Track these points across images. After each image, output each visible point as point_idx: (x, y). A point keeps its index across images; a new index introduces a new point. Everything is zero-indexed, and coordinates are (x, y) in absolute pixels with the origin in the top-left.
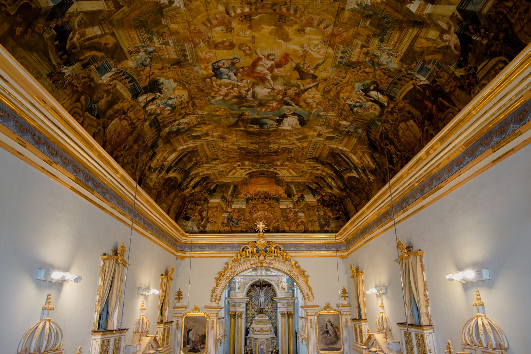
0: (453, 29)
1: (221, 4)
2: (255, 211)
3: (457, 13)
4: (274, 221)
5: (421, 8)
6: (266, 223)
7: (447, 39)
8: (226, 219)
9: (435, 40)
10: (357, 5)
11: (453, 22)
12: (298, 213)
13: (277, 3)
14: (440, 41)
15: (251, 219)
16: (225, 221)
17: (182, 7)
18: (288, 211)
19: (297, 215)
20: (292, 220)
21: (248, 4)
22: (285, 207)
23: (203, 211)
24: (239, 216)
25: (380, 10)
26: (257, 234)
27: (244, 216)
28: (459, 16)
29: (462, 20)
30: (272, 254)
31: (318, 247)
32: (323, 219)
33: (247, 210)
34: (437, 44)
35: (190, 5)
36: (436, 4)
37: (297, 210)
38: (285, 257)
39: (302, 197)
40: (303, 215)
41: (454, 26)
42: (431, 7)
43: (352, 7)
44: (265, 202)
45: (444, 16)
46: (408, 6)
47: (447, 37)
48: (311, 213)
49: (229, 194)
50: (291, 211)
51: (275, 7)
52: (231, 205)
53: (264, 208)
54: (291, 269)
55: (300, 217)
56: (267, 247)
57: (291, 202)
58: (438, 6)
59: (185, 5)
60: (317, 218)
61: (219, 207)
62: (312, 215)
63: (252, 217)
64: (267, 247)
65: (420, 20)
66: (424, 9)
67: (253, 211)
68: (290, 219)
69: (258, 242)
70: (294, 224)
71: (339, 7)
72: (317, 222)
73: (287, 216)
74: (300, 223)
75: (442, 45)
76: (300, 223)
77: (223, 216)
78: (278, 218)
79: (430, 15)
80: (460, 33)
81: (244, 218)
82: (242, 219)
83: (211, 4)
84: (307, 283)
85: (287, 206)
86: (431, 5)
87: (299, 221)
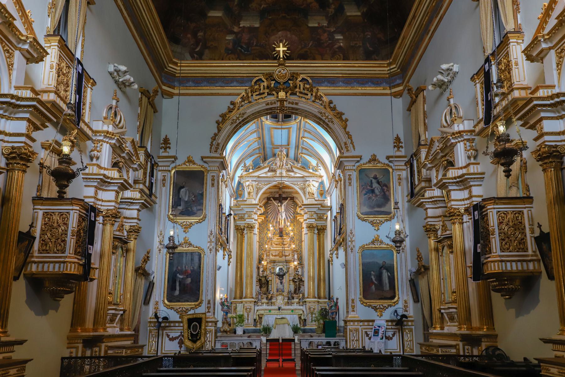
4: (300, 47)
6: (289, 46)
16: (230, 46)
19: (334, 37)
20: (326, 45)
26: (276, 61)
31: (362, 80)
37: (332, 30)
38: (314, 94)
39: (340, 10)
40: (342, 37)
44: (288, 17)
49: (236, 3)
52: (239, 22)
56: (289, 80)
57: (324, 18)
64: (289, 80)
69: (277, 72)
70: (328, 51)
72: (361, 49)
74: (337, 50)
76: (337, 50)
77: (227, 38)
82: (255, 44)
84: (345, 128)
85: (319, 24)
87: (336, 46)
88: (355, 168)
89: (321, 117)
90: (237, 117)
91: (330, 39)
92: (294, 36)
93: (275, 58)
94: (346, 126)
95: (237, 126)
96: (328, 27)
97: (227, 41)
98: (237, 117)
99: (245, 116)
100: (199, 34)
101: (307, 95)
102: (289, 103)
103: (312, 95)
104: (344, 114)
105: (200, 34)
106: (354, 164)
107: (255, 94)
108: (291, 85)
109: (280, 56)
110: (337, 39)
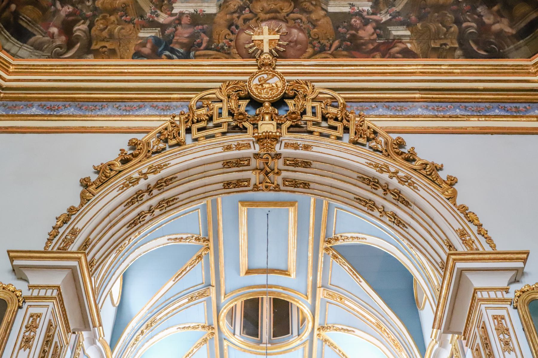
2: (246, 20)
8: (149, 46)
12: (390, 28)
15: (233, 44)
18: (356, 21)
19: (389, 32)
20: (371, 47)
22: (347, 9)
23: (76, 22)
24: (193, 36)
26: (253, 62)
27: (211, 37)
30: (305, 118)
32: (476, 42)
33: (222, 20)
48: (433, 27)
50: (366, 22)
53: (276, 12)
54: (381, 160)
55: (399, 39)
60: (455, 41)
61: (131, 11)
62: (438, 32)
63: (237, 40)
67: (240, 22)
68: (363, 44)
69: (256, 81)
73: (354, 38)
77: (141, 35)
78: (325, 42)
81: (210, 42)
82: (204, 45)
88: (511, 296)
89: (378, 174)
90: (141, 173)
91: (379, 36)
92: (295, 31)
93: (252, 56)
94: (455, 193)
95: (139, 195)
96: (373, 14)
97: (139, 41)
98: (141, 173)
99: (163, 173)
100: (76, 28)
101: (335, 128)
102: (287, 145)
103: (346, 130)
104: (441, 169)
105: (80, 28)
106: (504, 285)
107: (195, 127)
108: (291, 108)
109: (262, 51)
110: (398, 36)
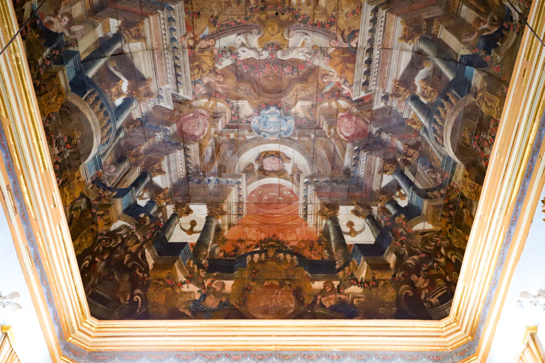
0: (67, 34)
1: (322, 8)
3: (76, 49)
5: (106, 27)
7: (63, 20)
9: (72, 5)
10: (172, 9)
11: (73, 39)
13: (261, 11)
14: (66, 11)
17: (365, 4)
21: (293, 9)
25: (145, 5)
28: (72, 49)
29: (67, 49)
34: (66, 5)
35: (355, 8)
36: (97, 40)
41: (68, 37)
42: (99, 35)
43: (177, 5)
45: (83, 36)
46: (120, 22)
47: (65, 20)
51: (262, 6)
58: (94, 40)
59: (361, 7)
65: (99, 14)
66: (104, 28)
71: (192, 4)
75: (62, 9)
79: (95, 26)
80: (59, 38)
83: (333, 7)
86: (101, 36)
